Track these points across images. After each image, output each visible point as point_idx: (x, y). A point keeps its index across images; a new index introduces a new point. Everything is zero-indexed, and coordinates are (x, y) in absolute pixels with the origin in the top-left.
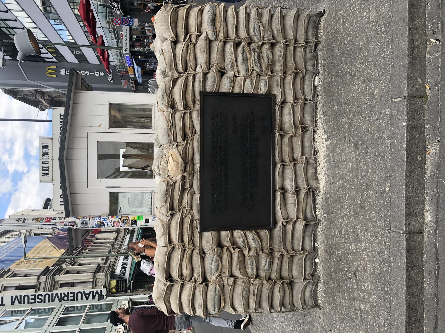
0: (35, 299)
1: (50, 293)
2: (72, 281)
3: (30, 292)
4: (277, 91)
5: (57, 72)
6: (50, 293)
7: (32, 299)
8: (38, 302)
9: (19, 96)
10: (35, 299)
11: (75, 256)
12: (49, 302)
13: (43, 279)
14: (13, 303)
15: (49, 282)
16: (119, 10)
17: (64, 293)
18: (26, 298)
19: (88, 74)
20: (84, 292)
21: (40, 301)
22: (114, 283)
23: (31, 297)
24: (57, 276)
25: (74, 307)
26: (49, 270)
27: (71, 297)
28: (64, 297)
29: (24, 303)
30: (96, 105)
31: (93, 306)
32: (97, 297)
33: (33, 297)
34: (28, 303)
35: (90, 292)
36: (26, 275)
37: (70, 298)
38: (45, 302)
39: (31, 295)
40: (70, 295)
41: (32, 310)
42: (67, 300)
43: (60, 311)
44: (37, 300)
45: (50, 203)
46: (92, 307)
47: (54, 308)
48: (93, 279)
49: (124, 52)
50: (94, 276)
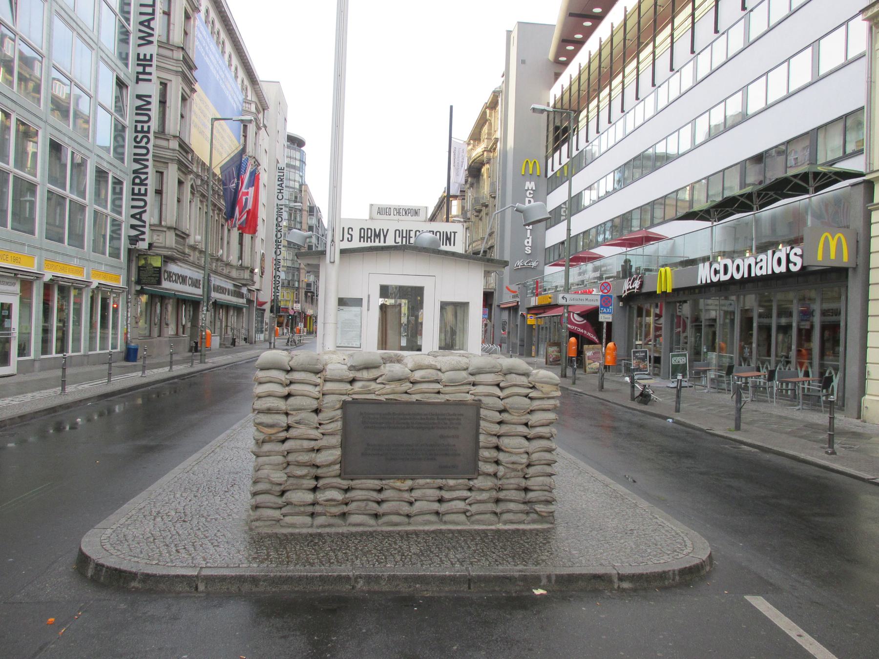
0: (142, 133)
1: (150, 157)
2: (164, 191)
3: (154, 125)
4: (479, 482)
5: (531, 177)
6: (150, 157)
7: (142, 127)
8: (137, 137)
9: (488, 111)
10: (142, 131)
11: (210, 199)
12: (135, 154)
14: (139, 97)
15: (168, 154)
16: (629, 289)
17: (147, 178)
18: (146, 118)
20: (145, 211)
21: (138, 140)
22: (157, 263)
25: (121, 193)
26: (187, 152)
27: (140, 189)
28: (140, 178)
29: (137, 114)
30: (468, 286)
31: (120, 225)
32: (134, 233)
33: (146, 129)
34: (137, 121)
35: (145, 222)
36: (182, 116)
37: (136, 188)
38: (135, 147)
39: (149, 127)
40: (143, 189)
41: (124, 127)
42: (134, 184)
43: (118, 173)
44: (140, 135)
45: (296, 146)
46: (116, 224)
47: (123, 162)
48: (166, 227)
49: (561, 296)
50: (169, 228)
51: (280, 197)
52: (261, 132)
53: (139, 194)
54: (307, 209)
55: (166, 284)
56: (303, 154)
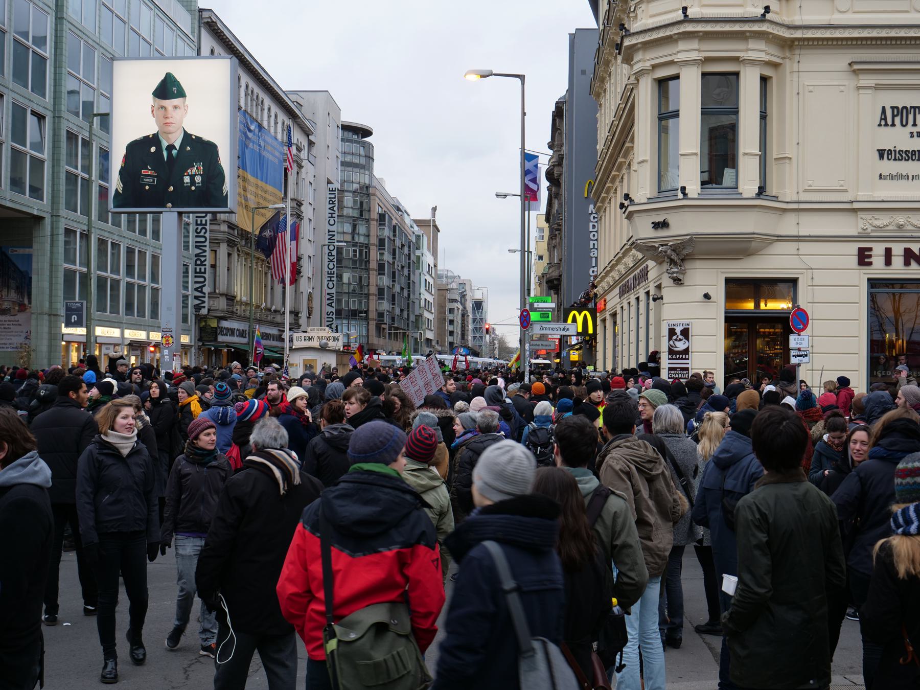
1: (207, 243)
6: (207, 243)
10: (201, 224)
13: (224, 228)
15: (220, 236)
19: (592, 255)
22: (214, 324)
23: (204, 220)
24: (225, 245)
32: (197, 302)
42: (196, 265)
44: (200, 227)
50: (222, 295)
51: (332, 222)
52: (303, 170)
53: (200, 272)
54: (376, 216)
55: (221, 338)
56: (369, 147)
